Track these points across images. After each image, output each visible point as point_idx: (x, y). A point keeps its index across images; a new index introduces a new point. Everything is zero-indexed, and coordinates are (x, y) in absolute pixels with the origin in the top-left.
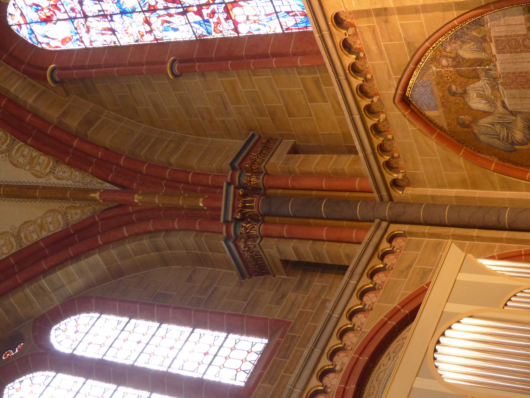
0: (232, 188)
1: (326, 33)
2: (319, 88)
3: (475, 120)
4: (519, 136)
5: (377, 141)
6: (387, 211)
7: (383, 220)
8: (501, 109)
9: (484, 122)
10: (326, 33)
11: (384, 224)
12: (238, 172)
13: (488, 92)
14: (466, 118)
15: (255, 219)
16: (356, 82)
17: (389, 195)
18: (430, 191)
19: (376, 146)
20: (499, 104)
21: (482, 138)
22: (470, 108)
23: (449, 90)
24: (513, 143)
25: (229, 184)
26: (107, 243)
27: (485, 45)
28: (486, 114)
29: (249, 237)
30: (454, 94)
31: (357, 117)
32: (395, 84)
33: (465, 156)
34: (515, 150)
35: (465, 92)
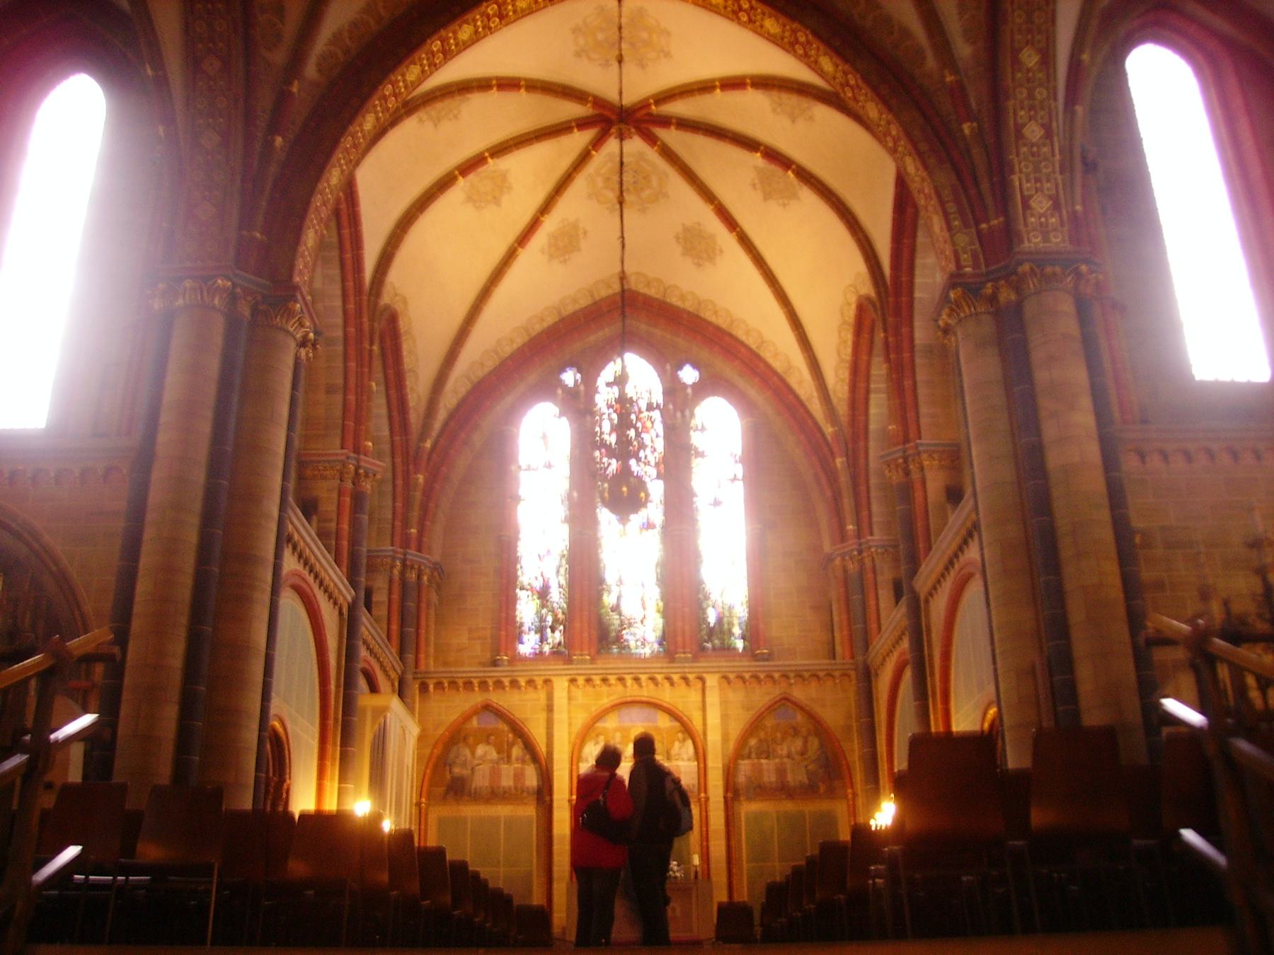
0: (425, 561)
1: (542, 673)
2: (479, 638)
3: (469, 746)
4: (457, 770)
5: (460, 682)
6: (409, 676)
7: (402, 673)
8: (476, 762)
9: (467, 752)
10: (542, 673)
11: (400, 672)
12: (431, 566)
13: (489, 757)
14: (471, 740)
15: (403, 573)
16: (506, 681)
17: (418, 678)
18: (417, 706)
19: (457, 680)
20: (480, 762)
21: (455, 748)
22: (478, 744)
23: (491, 734)
24: (450, 765)
25: (427, 559)
26: (392, 442)
27: (520, 761)
28: (473, 753)
29: (392, 567)
30: (488, 737)
31: (482, 674)
32: (500, 704)
33: (442, 735)
34: (445, 766)
35: (488, 743)
